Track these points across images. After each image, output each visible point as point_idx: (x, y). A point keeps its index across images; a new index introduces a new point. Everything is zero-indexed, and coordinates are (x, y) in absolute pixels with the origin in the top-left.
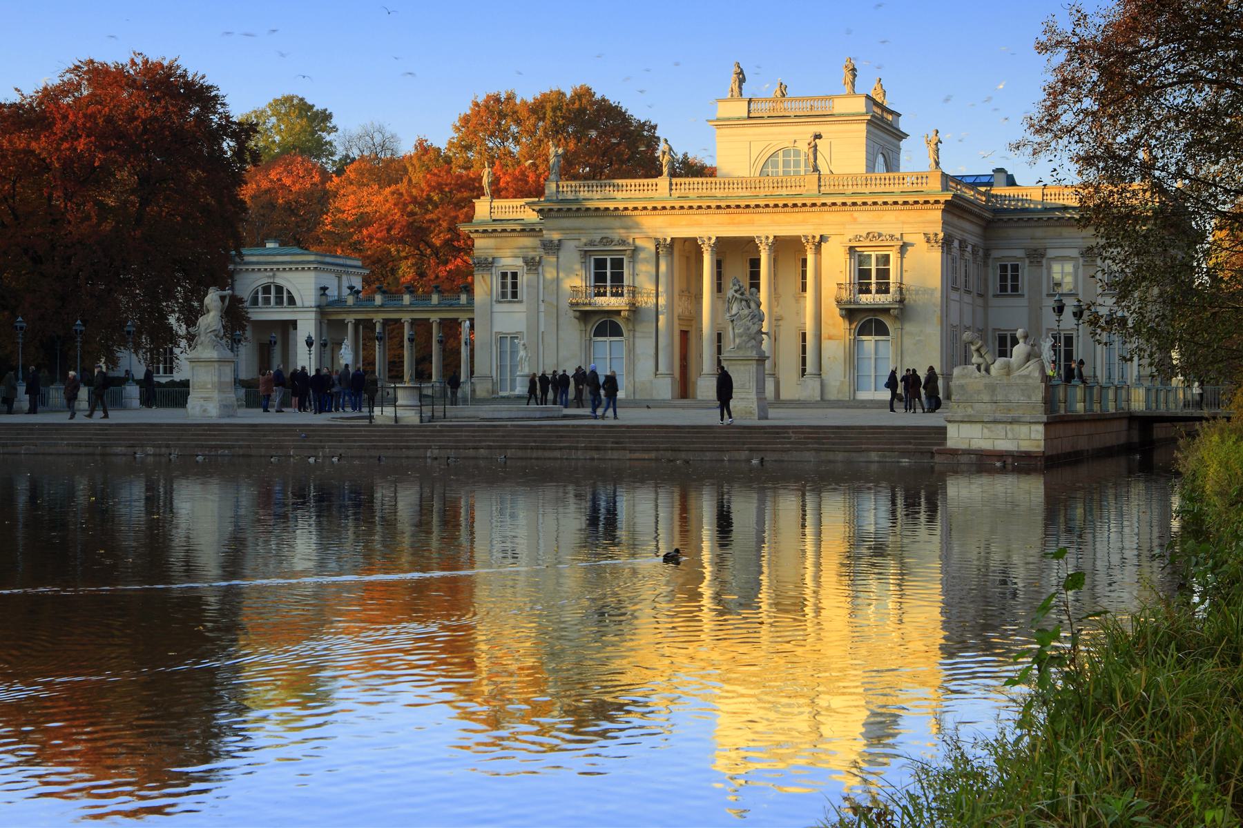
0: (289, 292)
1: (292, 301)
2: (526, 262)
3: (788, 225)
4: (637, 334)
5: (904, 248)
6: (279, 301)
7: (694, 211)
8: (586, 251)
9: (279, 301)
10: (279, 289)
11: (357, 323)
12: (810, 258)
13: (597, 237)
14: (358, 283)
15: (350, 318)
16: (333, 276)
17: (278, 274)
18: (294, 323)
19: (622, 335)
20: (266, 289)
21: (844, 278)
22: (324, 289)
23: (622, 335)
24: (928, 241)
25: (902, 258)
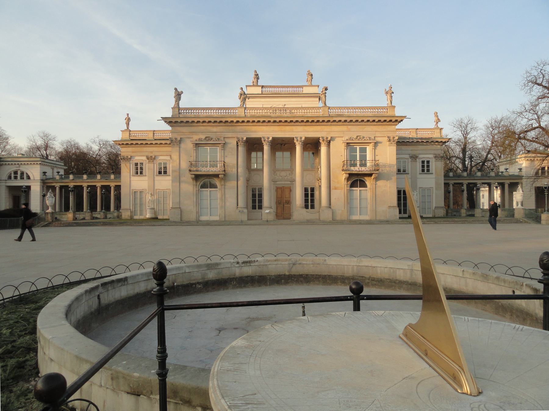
0: (27, 174)
1: (29, 178)
2: (148, 159)
3: (312, 132)
4: (226, 187)
5: (376, 144)
6: (22, 178)
7: (260, 124)
8: (196, 144)
9: (22, 178)
10: (22, 173)
11: (61, 188)
12: (323, 149)
13: (203, 137)
14: (62, 172)
15: (57, 185)
16: (50, 168)
17: (21, 166)
18: (29, 188)
19: (217, 188)
20: (16, 173)
21: (344, 158)
22: (45, 173)
23: (217, 188)
24: (390, 141)
25: (375, 149)
